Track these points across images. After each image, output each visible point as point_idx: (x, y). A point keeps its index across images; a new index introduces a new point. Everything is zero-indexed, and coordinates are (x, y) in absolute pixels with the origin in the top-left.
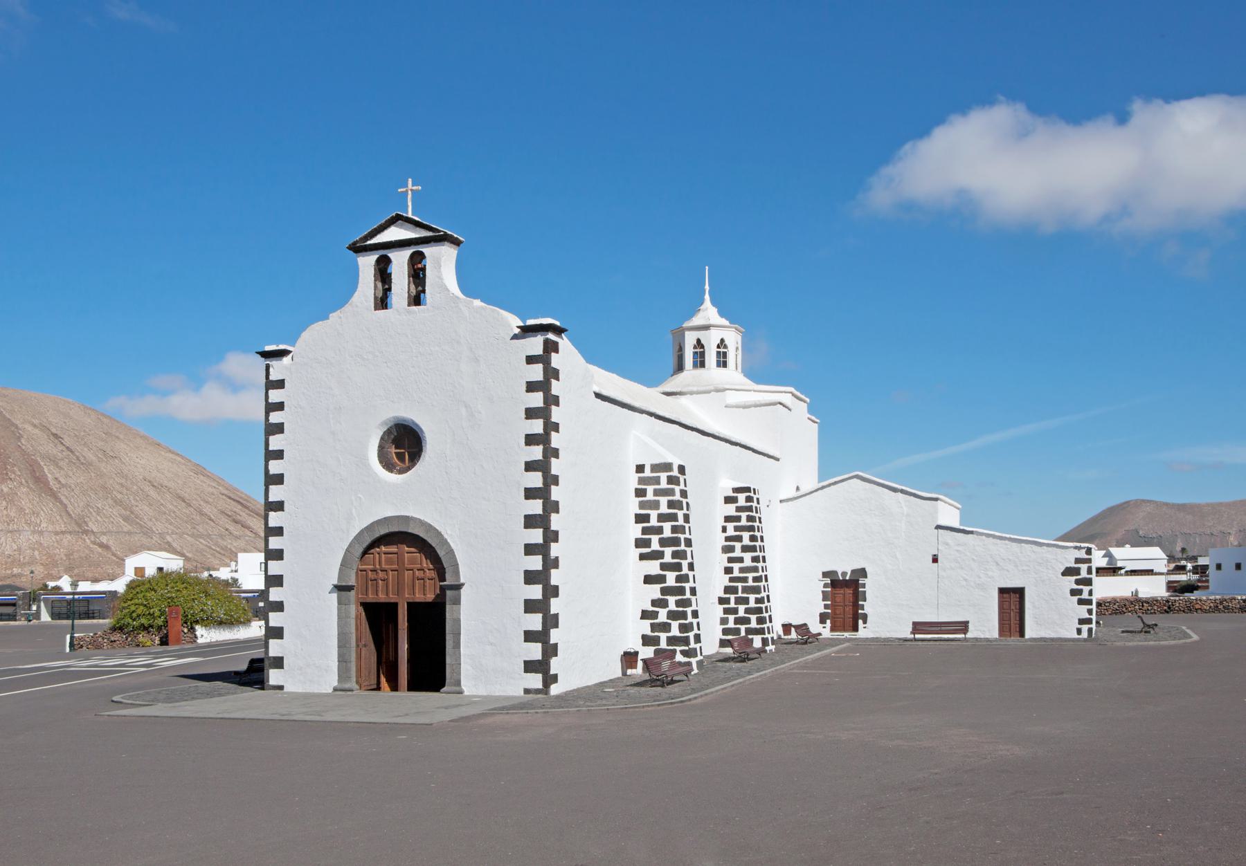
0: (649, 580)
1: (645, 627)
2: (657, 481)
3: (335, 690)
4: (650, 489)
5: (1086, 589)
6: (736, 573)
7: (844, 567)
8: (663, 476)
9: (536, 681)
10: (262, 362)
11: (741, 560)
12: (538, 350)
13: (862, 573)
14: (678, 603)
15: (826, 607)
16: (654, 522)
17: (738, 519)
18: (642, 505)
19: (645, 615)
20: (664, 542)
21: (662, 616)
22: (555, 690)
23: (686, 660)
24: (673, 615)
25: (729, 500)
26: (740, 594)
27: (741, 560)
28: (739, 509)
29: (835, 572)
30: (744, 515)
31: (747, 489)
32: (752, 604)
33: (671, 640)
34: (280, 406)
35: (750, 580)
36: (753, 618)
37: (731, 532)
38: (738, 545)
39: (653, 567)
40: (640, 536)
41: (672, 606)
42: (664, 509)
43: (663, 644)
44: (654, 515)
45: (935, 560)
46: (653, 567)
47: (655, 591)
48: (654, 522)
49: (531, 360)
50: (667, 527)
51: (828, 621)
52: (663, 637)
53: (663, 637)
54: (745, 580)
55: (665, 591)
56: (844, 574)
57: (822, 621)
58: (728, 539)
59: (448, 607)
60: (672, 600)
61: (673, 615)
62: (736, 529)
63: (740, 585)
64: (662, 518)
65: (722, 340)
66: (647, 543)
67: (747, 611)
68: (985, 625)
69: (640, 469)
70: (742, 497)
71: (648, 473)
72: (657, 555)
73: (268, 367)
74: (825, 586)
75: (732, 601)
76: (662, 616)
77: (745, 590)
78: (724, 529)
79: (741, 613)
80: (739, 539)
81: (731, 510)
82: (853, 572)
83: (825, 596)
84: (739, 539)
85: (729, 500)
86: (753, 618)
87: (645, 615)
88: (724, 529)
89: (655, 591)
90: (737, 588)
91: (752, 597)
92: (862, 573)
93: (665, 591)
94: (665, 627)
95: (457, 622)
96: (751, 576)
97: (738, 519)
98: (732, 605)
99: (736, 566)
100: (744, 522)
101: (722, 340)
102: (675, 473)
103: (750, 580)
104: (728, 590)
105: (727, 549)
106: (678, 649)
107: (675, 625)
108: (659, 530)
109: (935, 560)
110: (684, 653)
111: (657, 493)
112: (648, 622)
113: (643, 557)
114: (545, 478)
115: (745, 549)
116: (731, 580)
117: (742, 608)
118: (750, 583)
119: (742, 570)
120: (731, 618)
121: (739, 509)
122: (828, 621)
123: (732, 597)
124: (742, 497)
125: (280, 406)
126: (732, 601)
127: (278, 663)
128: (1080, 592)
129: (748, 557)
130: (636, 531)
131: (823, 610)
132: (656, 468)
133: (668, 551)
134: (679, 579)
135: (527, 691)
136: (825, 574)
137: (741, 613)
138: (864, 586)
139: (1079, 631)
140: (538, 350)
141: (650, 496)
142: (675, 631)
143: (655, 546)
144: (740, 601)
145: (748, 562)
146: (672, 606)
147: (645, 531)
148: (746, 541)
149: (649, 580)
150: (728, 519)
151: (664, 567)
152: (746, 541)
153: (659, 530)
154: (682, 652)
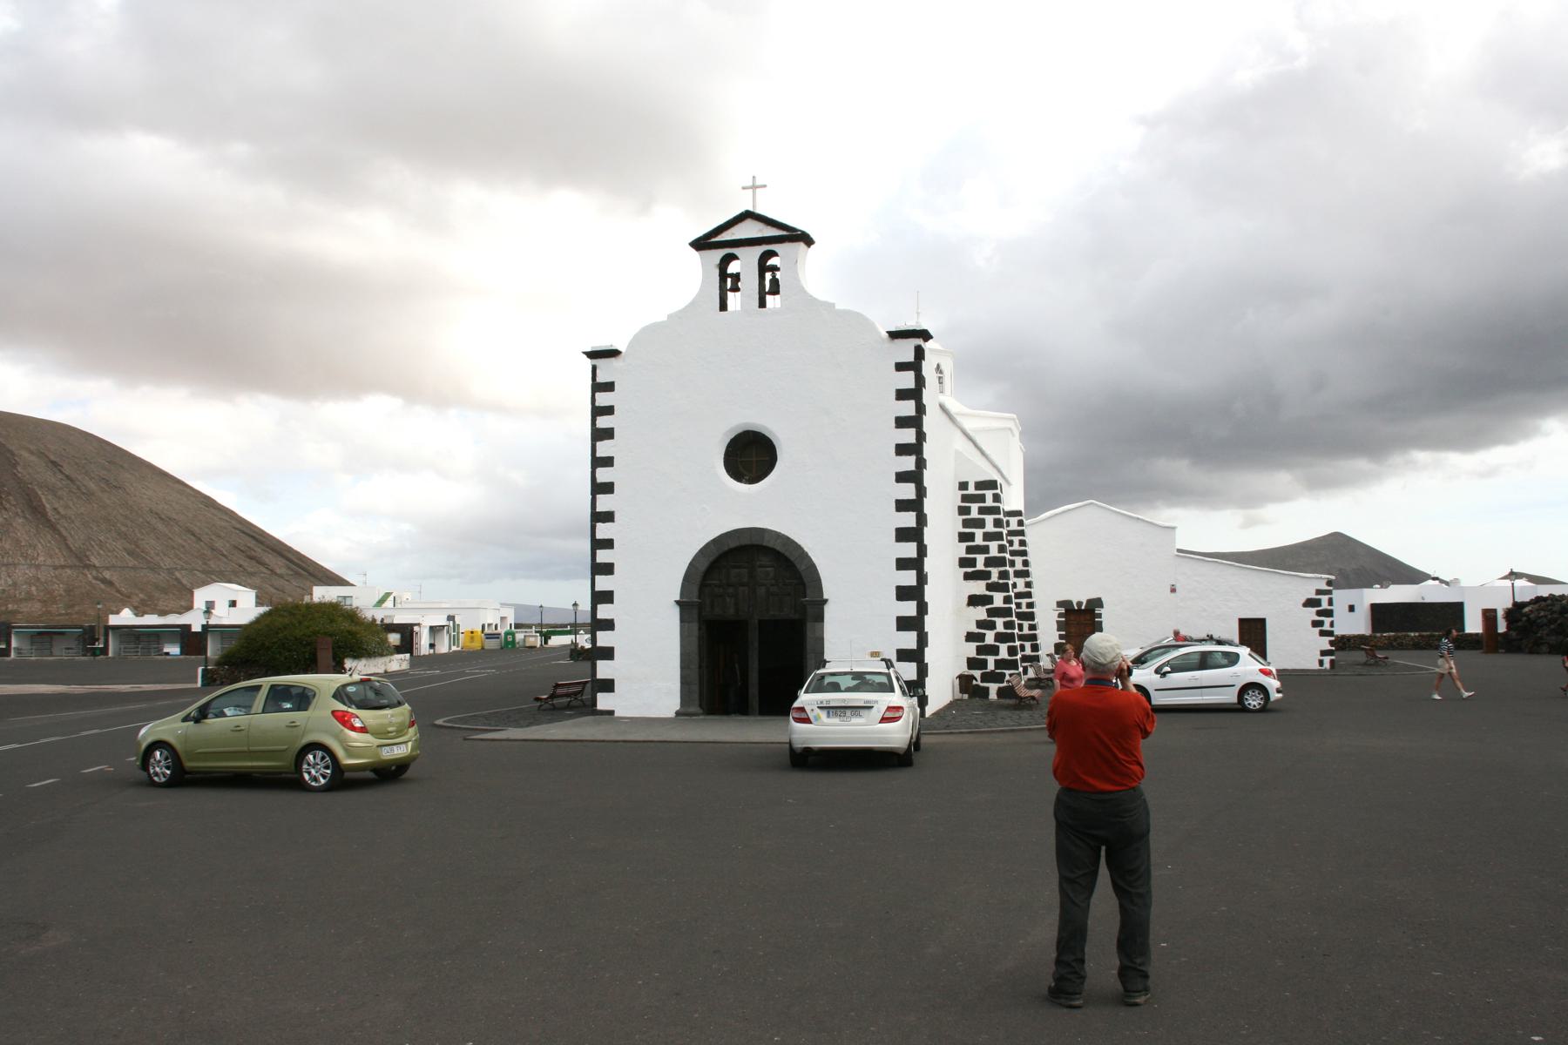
0: (974, 601)
1: (971, 649)
2: (982, 498)
3: (678, 713)
4: (975, 507)
5: (1327, 621)
7: (1080, 596)
10: (588, 363)
12: (910, 357)
13: (1096, 603)
15: (1061, 637)
16: (979, 540)
18: (966, 523)
19: (970, 637)
20: (990, 562)
21: (990, 638)
24: (1001, 638)
29: (1070, 602)
34: (609, 410)
36: (1028, 645)
39: (979, 588)
40: (964, 555)
41: (1000, 628)
43: (991, 666)
44: (979, 533)
45: (1173, 590)
46: (979, 588)
47: (981, 613)
48: (979, 541)
49: (900, 367)
50: (993, 546)
52: (991, 660)
53: (991, 660)
55: (991, 612)
56: (1079, 604)
59: (809, 625)
60: (1000, 622)
61: (1001, 638)
64: (988, 537)
66: (972, 563)
71: (971, 490)
72: (983, 575)
73: (594, 369)
74: (1060, 615)
76: (990, 638)
82: (1089, 601)
83: (1060, 626)
87: (970, 637)
89: (981, 613)
92: (1096, 603)
93: (994, 612)
94: (993, 650)
106: (1007, 672)
108: (985, 550)
109: (1173, 590)
111: (982, 511)
112: (974, 645)
113: (967, 577)
118: (1024, 609)
125: (609, 410)
127: (608, 686)
128: (1320, 624)
130: (961, 550)
132: (979, 485)
133: (995, 572)
136: (1060, 604)
138: (1100, 616)
139: (1321, 663)
140: (910, 357)
142: (1003, 653)
143: (980, 566)
145: (1021, 588)
146: (1000, 628)
147: (969, 550)
149: (974, 601)
151: (990, 587)
153: (985, 550)
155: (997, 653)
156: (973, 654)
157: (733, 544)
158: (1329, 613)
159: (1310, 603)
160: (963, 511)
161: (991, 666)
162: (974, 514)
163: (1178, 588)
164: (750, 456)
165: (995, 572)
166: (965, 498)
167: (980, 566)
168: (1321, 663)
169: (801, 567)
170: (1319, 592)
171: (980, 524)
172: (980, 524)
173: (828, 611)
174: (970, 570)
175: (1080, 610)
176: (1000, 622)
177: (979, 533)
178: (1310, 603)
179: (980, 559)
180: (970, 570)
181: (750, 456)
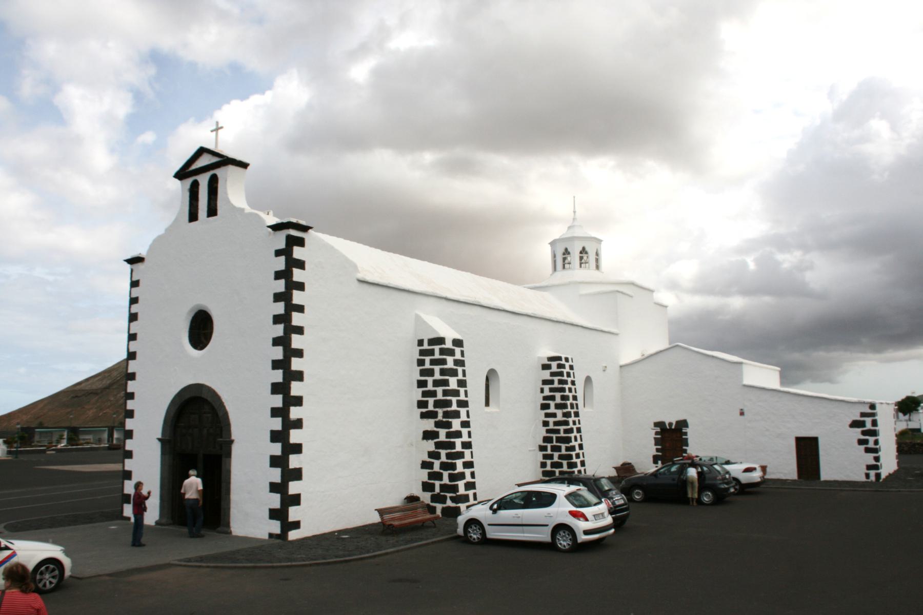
0: (428, 435)
4: (427, 359)
6: (551, 426)
7: (670, 418)
8: (437, 348)
9: (275, 527)
11: (554, 415)
13: (683, 424)
14: (449, 456)
15: (657, 450)
16: (430, 387)
17: (552, 382)
20: (438, 404)
22: (293, 535)
23: (453, 505)
24: (444, 466)
25: (545, 367)
26: (555, 443)
27: (554, 415)
28: (553, 374)
30: (556, 379)
31: (559, 358)
32: (564, 452)
33: (444, 488)
35: (562, 431)
36: (565, 463)
37: (547, 393)
38: (552, 404)
39: (429, 425)
41: (443, 458)
42: (437, 376)
43: (437, 490)
44: (430, 380)
45: (742, 414)
46: (429, 425)
47: (430, 445)
48: (430, 387)
49: (278, 253)
51: (660, 462)
54: (558, 431)
55: (439, 445)
56: (670, 424)
57: (655, 462)
58: (545, 398)
59: (223, 459)
60: (443, 453)
61: (444, 466)
62: (551, 390)
63: (554, 436)
64: (437, 383)
65: (584, 248)
67: (560, 457)
68: (786, 467)
69: (420, 343)
70: (554, 364)
71: (426, 346)
74: (657, 433)
75: (549, 448)
77: (559, 440)
78: (542, 391)
79: (556, 459)
80: (552, 398)
81: (546, 375)
82: (678, 423)
83: (657, 442)
84: (552, 398)
85: (545, 367)
86: (565, 463)
88: (542, 391)
89: (430, 445)
90: (552, 438)
91: (563, 446)
92: (683, 424)
93: (439, 445)
94: (439, 476)
95: (229, 472)
96: (562, 428)
97: (552, 382)
98: (549, 452)
99: (551, 420)
100: (556, 385)
101: (584, 248)
102: (449, 345)
103: (562, 431)
104: (547, 440)
105: (545, 407)
106: (449, 495)
107: (446, 474)
108: (433, 394)
109: (742, 414)
110: (453, 500)
112: (426, 471)
113: (424, 416)
114: (285, 351)
115: (558, 406)
116: (548, 431)
117: (556, 455)
118: (562, 434)
119: (556, 423)
120: (549, 462)
121: (553, 374)
122: (660, 462)
123: (549, 445)
124: (554, 364)
126: (549, 448)
129: (559, 413)
131: (656, 453)
132: (433, 342)
133: (440, 412)
134: (449, 435)
135: (271, 535)
136: (657, 424)
137: (556, 459)
138: (686, 434)
140: (282, 245)
141: (427, 365)
143: (431, 407)
144: (555, 449)
145: (560, 417)
147: (425, 394)
148: (558, 400)
149: (428, 435)
150: (545, 382)
151: (438, 424)
152: (558, 400)
154: (451, 498)
155: (441, 479)
156: (426, 479)
157: (187, 396)
158: (874, 433)
159: (855, 424)
160: (421, 363)
161: (437, 490)
162: (427, 365)
163: (745, 411)
164: (201, 329)
165: (440, 412)
166: (422, 353)
167: (431, 407)
168: (867, 476)
169: (220, 414)
170: (863, 415)
171: (430, 373)
172: (430, 373)
173: (235, 449)
174: (424, 410)
175: (671, 429)
176: (443, 453)
177: (430, 380)
178: (855, 424)
179: (431, 401)
180: (424, 410)
181: (201, 329)
